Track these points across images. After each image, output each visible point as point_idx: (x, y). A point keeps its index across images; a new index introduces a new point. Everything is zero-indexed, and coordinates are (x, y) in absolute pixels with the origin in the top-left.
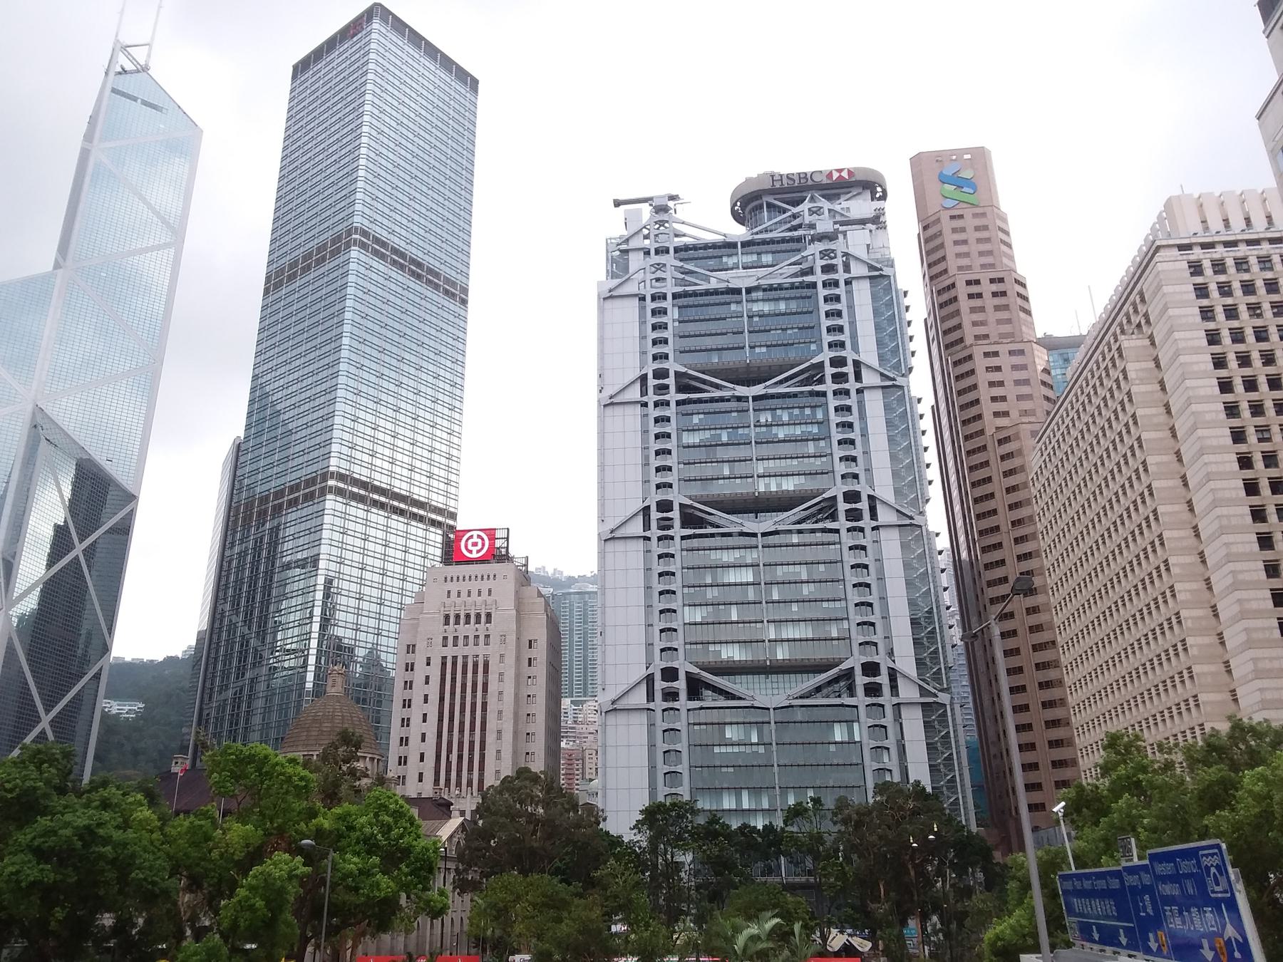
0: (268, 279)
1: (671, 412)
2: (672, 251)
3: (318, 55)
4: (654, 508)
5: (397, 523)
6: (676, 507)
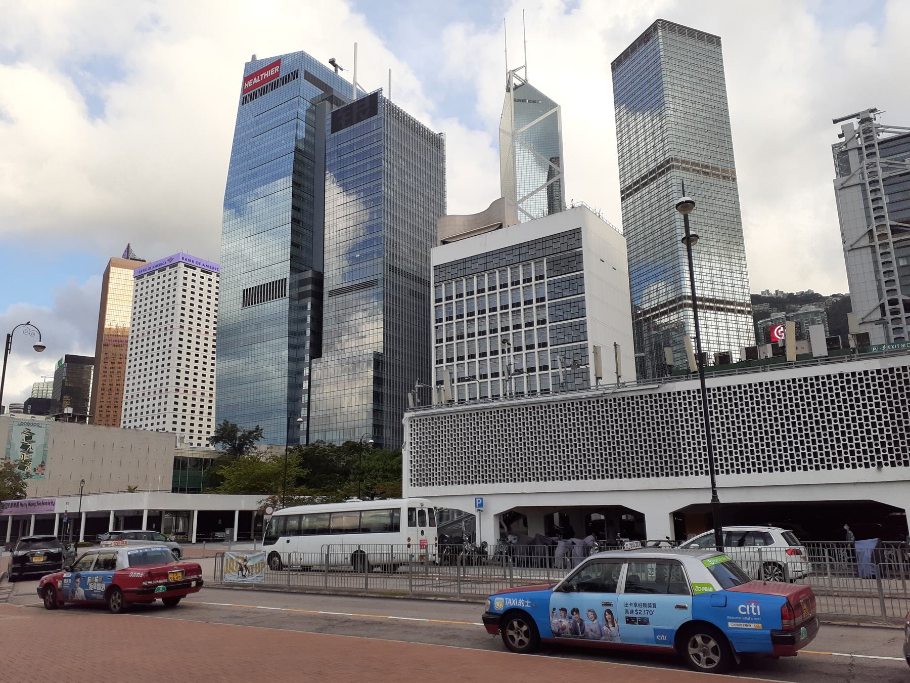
0: (622, 192)
1: (891, 248)
2: (876, 145)
3: (625, 55)
4: (887, 304)
5: (721, 316)
6: (901, 302)
